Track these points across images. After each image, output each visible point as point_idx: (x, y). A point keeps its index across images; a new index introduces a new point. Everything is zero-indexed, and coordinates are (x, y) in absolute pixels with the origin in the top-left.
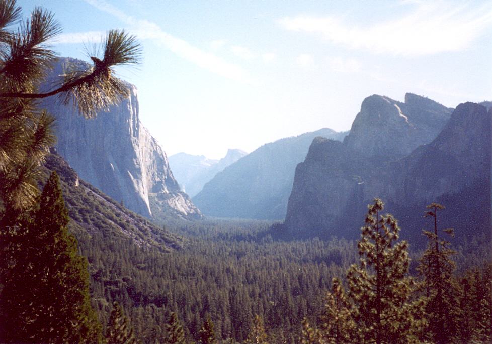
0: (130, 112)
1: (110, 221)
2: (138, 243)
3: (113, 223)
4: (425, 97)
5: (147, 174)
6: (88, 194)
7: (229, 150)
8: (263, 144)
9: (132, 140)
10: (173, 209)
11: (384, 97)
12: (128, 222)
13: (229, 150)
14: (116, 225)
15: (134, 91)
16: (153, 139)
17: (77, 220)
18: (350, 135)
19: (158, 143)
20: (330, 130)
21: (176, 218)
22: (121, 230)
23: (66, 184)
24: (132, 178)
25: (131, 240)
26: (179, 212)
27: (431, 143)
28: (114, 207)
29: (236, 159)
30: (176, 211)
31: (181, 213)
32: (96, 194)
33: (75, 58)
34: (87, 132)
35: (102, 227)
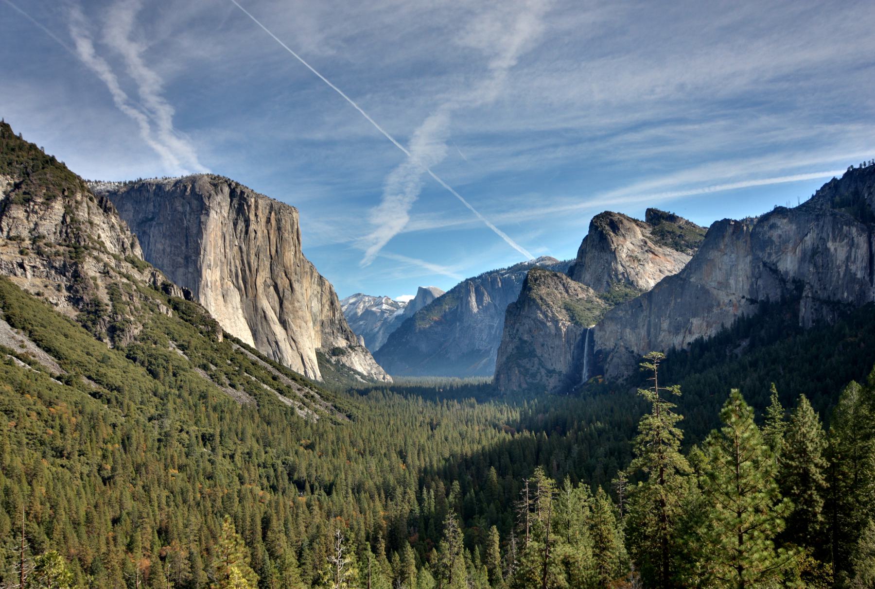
0: (289, 243)
1: (265, 386)
2: (301, 413)
3: (269, 389)
4: (671, 213)
5: (314, 323)
6: (237, 351)
7: (420, 289)
8: (463, 280)
9: (293, 279)
10: (350, 369)
11: (619, 214)
12: (289, 387)
13: (420, 289)
14: (273, 391)
15: (294, 214)
16: (321, 277)
18: (576, 265)
19: (327, 283)
20: (550, 259)
21: (353, 380)
22: (281, 398)
23: (206, 339)
24: (295, 329)
25: (293, 409)
27: (680, 273)
28: (270, 368)
29: (429, 301)
30: (353, 370)
31: (359, 374)
32: (246, 352)
33: (216, 175)
35: (255, 395)
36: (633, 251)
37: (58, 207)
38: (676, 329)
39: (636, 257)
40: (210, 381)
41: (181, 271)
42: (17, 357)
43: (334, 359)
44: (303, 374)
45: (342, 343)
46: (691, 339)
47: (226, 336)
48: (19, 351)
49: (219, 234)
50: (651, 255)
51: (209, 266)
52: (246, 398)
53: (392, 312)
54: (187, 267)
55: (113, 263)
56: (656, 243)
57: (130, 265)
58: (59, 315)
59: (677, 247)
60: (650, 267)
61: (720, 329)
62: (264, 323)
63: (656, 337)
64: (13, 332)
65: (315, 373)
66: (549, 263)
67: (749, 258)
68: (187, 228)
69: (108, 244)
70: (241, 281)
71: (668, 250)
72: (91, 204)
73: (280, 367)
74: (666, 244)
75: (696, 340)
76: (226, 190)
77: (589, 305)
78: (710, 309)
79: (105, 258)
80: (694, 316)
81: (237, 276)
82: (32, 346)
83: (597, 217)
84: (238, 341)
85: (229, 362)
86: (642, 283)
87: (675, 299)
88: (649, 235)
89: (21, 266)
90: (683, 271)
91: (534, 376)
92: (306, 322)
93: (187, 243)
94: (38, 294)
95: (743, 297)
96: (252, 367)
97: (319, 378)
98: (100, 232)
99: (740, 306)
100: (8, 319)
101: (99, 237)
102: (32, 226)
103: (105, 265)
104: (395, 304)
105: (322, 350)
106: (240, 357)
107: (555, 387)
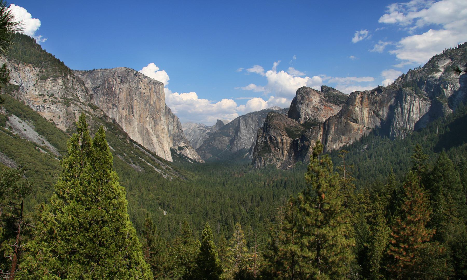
10: (186, 157)
12: (159, 164)
17: (130, 163)
20: (278, 107)
26: (188, 158)
28: (151, 155)
31: (190, 159)
34: (135, 110)
35: (144, 167)
36: (316, 105)
37: (60, 81)
38: (334, 140)
39: (317, 108)
40: (124, 160)
41: (111, 110)
42: (41, 148)
43: (178, 151)
44: (164, 158)
45: (182, 145)
46: (341, 145)
47: (131, 140)
48: (42, 145)
49: (128, 94)
50: (323, 107)
51: (123, 109)
52: (140, 169)
53: (204, 131)
54: (113, 109)
55: (82, 106)
56: (326, 101)
57: (89, 107)
58: (59, 129)
59: (336, 104)
60: (322, 113)
61: (354, 141)
62: (147, 135)
63: (326, 143)
64: (40, 137)
65: (170, 159)
66: (277, 109)
67: (367, 109)
68: (115, 91)
69: (80, 98)
70: (137, 116)
71: (331, 105)
72: (74, 80)
73: (154, 155)
74: (330, 102)
75: (344, 146)
76: (132, 74)
77: (296, 129)
78: (350, 131)
79: (79, 103)
80: (343, 135)
81: (136, 113)
82: (47, 143)
83: (299, 89)
84: (135, 143)
85: (133, 152)
86: (320, 120)
87: (335, 127)
88: (323, 97)
89: (43, 107)
90: (338, 114)
91: (270, 161)
92: (166, 135)
93: (114, 97)
94: (50, 120)
95: (365, 126)
96: (143, 155)
97: (172, 161)
98: (77, 93)
99: (363, 130)
100: (37, 130)
101: (77, 95)
102: (49, 89)
103: (80, 107)
104: (207, 127)
105: (173, 148)
106: (137, 151)
107: (280, 167)
